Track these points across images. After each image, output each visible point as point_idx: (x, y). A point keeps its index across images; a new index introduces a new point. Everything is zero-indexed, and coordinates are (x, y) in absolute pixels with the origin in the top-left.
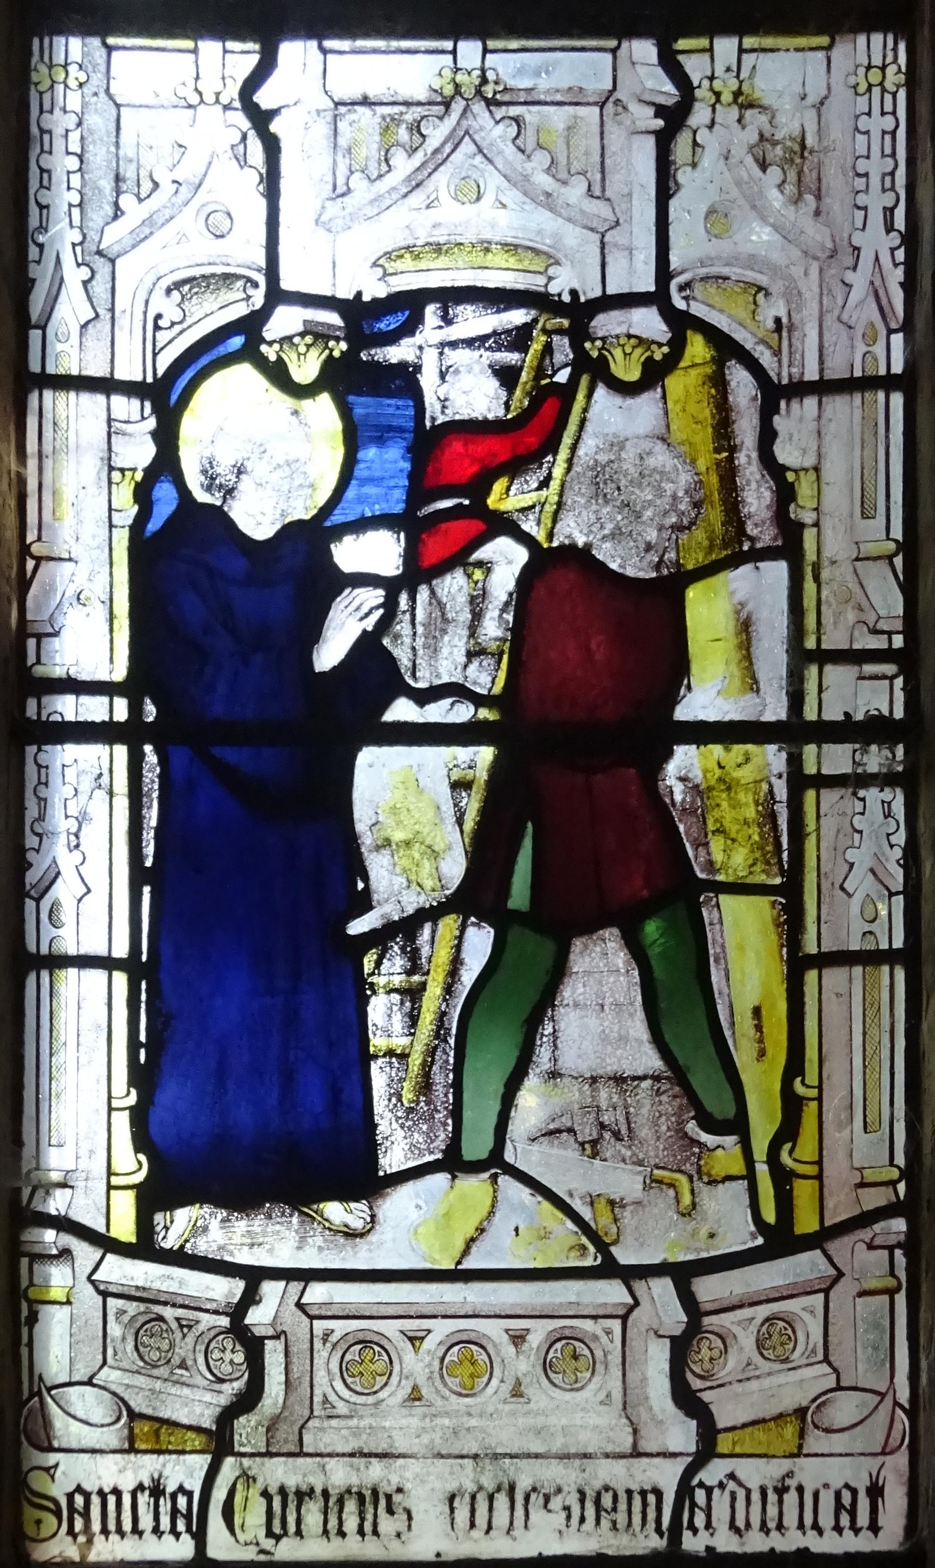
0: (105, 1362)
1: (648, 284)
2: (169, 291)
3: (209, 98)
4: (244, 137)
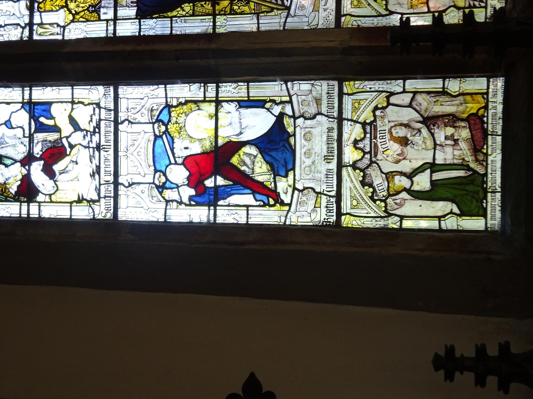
0: (307, 211)
1: (152, 125)
2: (153, 199)
3: (126, 193)
4: (132, 188)
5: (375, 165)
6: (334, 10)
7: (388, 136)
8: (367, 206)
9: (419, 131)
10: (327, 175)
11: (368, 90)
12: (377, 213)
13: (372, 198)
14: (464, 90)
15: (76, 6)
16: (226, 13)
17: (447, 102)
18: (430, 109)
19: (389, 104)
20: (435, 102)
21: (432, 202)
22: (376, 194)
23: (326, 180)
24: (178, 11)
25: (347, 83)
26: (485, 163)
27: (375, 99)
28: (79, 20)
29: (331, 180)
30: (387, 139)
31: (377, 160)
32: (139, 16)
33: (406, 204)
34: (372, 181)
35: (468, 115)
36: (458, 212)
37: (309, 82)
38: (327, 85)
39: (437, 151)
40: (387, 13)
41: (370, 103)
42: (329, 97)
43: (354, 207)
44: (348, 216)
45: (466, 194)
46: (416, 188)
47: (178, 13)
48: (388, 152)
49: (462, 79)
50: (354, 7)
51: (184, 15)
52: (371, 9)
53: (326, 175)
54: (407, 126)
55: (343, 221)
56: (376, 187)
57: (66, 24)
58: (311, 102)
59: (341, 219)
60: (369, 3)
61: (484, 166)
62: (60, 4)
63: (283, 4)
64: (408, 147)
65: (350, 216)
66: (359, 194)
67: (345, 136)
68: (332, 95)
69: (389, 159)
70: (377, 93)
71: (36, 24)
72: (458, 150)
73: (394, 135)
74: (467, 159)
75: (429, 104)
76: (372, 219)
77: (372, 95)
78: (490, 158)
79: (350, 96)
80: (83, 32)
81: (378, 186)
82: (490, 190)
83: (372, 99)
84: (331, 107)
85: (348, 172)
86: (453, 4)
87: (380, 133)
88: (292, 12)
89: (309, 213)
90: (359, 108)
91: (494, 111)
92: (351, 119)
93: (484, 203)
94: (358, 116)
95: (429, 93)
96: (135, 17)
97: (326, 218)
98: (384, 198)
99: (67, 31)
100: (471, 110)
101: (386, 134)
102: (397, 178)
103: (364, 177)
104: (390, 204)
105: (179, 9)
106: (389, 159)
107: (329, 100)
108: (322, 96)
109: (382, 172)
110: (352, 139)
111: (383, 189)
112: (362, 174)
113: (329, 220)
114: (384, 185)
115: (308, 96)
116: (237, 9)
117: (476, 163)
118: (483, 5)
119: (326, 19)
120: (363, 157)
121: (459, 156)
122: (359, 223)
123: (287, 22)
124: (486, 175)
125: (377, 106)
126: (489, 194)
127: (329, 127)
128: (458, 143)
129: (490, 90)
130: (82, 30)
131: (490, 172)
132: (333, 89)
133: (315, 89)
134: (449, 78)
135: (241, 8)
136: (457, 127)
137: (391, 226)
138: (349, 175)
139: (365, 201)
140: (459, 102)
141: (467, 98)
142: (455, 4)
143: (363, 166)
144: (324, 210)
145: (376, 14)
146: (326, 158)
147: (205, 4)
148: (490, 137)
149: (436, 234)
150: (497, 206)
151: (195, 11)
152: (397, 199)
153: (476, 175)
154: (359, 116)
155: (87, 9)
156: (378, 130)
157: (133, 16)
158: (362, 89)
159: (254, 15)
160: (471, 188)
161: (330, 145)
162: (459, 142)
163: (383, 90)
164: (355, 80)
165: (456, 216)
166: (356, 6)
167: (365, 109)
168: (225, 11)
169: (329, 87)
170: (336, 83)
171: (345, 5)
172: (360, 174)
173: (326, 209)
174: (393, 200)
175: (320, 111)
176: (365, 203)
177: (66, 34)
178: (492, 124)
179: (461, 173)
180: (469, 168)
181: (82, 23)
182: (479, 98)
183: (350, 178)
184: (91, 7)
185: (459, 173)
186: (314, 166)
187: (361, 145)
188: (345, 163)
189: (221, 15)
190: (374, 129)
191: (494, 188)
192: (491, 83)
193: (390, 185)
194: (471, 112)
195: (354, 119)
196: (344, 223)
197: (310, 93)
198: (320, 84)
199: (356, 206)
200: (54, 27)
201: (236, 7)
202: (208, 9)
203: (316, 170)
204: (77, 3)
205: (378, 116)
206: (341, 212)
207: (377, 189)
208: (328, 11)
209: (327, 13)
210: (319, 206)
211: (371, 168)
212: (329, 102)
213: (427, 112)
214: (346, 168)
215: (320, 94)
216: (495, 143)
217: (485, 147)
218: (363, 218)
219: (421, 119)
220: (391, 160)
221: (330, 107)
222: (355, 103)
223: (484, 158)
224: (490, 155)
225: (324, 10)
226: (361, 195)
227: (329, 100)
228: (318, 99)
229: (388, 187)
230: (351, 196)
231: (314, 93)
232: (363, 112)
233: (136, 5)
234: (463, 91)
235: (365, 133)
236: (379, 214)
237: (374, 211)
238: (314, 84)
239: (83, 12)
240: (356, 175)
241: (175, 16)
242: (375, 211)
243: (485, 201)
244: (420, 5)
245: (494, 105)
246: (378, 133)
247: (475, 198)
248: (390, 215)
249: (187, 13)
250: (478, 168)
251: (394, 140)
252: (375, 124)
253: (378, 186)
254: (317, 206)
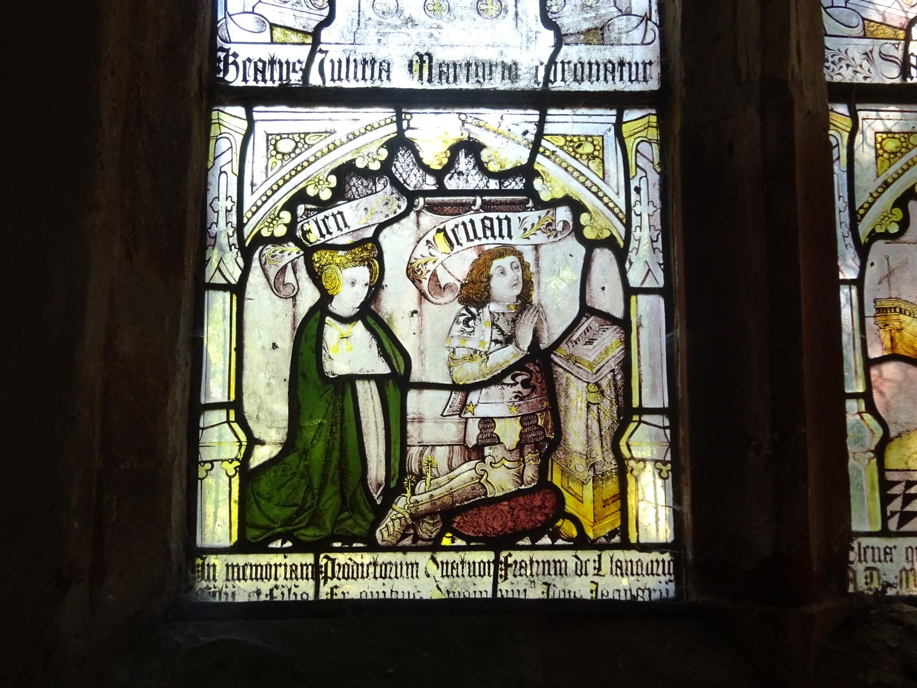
5: (404, 207)
7: (490, 244)
8: (276, 183)
9: (509, 339)
10: (373, 61)
11: (634, 184)
12: (254, 214)
13: (301, 196)
14: (635, 473)
17: (599, 421)
18: (575, 370)
19: (590, 246)
20: (597, 384)
21: (287, 383)
22: (311, 210)
23: (355, 61)
25: (654, 119)
26: (407, 542)
27: (606, 205)
29: (355, 74)
30: (484, 241)
31: (418, 213)
33: (280, 302)
34: (355, 199)
35: (560, 486)
36: (254, 463)
37: (654, 7)
38: (647, 61)
39: (445, 394)
40: (863, 239)
41: (594, 189)
42: (610, 66)
43: (273, 142)
44: (244, 125)
45: (309, 487)
46: (332, 331)
48: (444, 246)
49: (669, 466)
50: (879, 139)
52: (872, 190)
53: (373, 59)
54: (524, 301)
55: (229, 109)
56: (335, 210)
58: (593, 14)
59: (233, 103)
60: (892, 183)
61: (398, 541)
64: (459, 307)
65: (244, 132)
66: (312, 159)
67: (490, 116)
68: (617, 74)
69: (422, 249)
70: (624, 210)
72: (450, 459)
73: (497, 263)
74: (421, 486)
75: (591, 366)
76: (235, 199)
77: (618, 194)
78: (423, 559)
79: (613, 128)
81: (339, 217)
82: (325, 561)
83: (605, 195)
84: (579, 73)
85: (380, 126)
86: (893, 433)
87: (500, 220)
89: (253, 7)
90: (578, 156)
91: (571, 565)
92: (545, 132)
93: (283, 543)
94: (553, 152)
95: (626, 365)
97: (240, 61)
98: (299, 234)
100: (574, 495)
101: (499, 240)
102: (362, 274)
103: (366, 173)
104: (282, 252)
106: (422, 249)
107: (602, 67)
108: (612, 45)
109: (381, 227)
110: (481, 136)
111: (329, 233)
112: (375, 166)
113: (232, 68)
114: (340, 233)
115: (612, 4)
117: (407, 516)
118: (893, 525)
120: (427, 169)
121: (430, 464)
122: (223, 160)
124: (373, 546)
125: (585, 209)
126: (309, 558)
127: (519, 67)
128: (470, 460)
129: (634, 555)
131: (380, 562)
132: (633, 78)
133: (635, 25)
134: (673, 427)
136: (522, 455)
137: (214, 256)
138: (373, 128)
139: (292, 177)
140: (599, 458)
141: (610, 482)
142: (892, 440)
143: (401, 171)
144: (265, 53)
145: (858, 205)
146: (426, 58)
148: (488, 556)
149: (179, 396)
150: (272, 582)
152: (298, 274)
153: (371, 517)
154: (553, 157)
156: (510, 215)
158: (637, 166)
160: (330, 502)
161: (465, 72)
162: (473, 463)
163: (633, 229)
164: (663, 143)
165: (240, 457)
166: (882, 148)
167: (576, 174)
169: (641, 67)
170: (654, 85)
171: (883, 115)
172: (374, 160)
173: (266, 59)
174: (292, 261)
175: (568, 40)
176: (283, 178)
178: (531, 562)
179: (376, 470)
180: (392, 492)
182: (611, 522)
183: (363, 131)
185: (379, 462)
186: (399, 22)
187: (464, 163)
188: (408, 117)
190: (512, 203)
191: (330, 574)
192: (655, 555)
193: (341, 253)
194: (566, 494)
195: (544, 143)
196: (222, 116)
197: (620, 11)
198: (649, 39)
199: (275, 149)
203: (388, 30)
205: (554, 214)
206: (256, 105)
207: (328, 213)
208: (865, 64)
209: (858, 61)
210: (275, 40)
211: (392, 194)
212: (594, 67)
213: (568, 360)
214: (394, 119)
215: (619, 40)
216: (472, 575)
217: (459, 542)
218: (236, 171)
219: (545, 344)
220: (417, 255)
221: (581, 70)
222: (592, 143)
223: (424, 540)
224: (433, 559)
225: (866, 54)
226: (310, 164)
227: (602, 67)
228: (602, 34)
229: (336, 248)
230: (308, 134)
231: (621, 23)
232: (566, 169)
234: (632, 470)
235: (502, 176)
236: (249, 220)
237: (259, 203)
238: (649, 22)
240: (373, 149)
242: (259, 208)
243: (288, 544)
244: (888, 337)
245: (591, 566)
246: (502, 215)
247: (298, 513)
248: (247, 253)
250: (392, 520)
251: (481, 262)
252: (531, 204)
253: (339, 217)
254: (278, 33)
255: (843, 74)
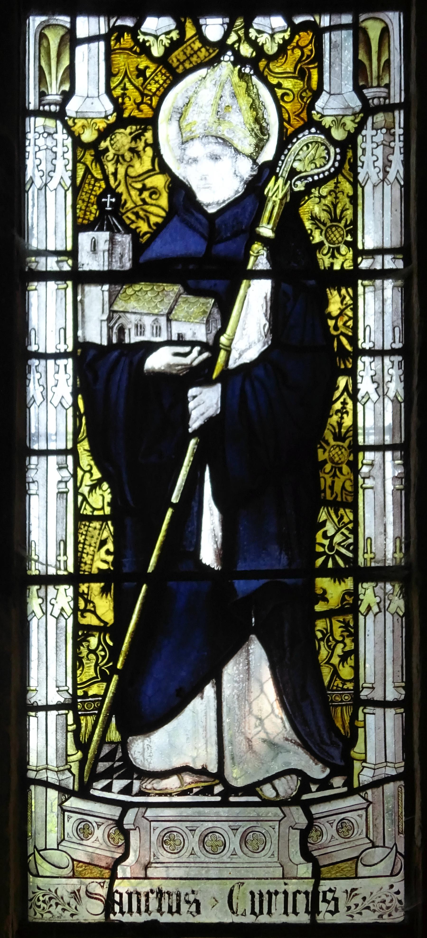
6: (75, 917)
15: (121, 152)
16: (79, 613)
24: (90, 471)
28: (80, 161)
32: (82, 353)
47: (85, 472)
51: (80, 491)
57: (70, 123)
62: (127, 99)
63: (95, 777)
71: (73, 23)
80: (44, 178)
88: (73, 803)
96: (81, 340)
99: (50, 123)
105: (97, 475)
116: (88, 646)
119: (50, 899)
123: (49, 790)
130: (52, 174)
135: (92, 656)
147: (108, 552)
151: (90, 522)
155: (109, 190)
157: (83, 333)
159: (68, 696)
168: (85, 610)
177: (40, 121)
181: (70, 174)
184: (113, 200)
189: (75, 599)
200: (62, 83)
201: (93, 641)
202: (92, 560)
204: (128, 155)
208: (73, 902)
209: (67, 899)
233: (115, 341)
239: (100, 176)
241: (77, 463)
249: (85, 499)
255: (52, 912)
